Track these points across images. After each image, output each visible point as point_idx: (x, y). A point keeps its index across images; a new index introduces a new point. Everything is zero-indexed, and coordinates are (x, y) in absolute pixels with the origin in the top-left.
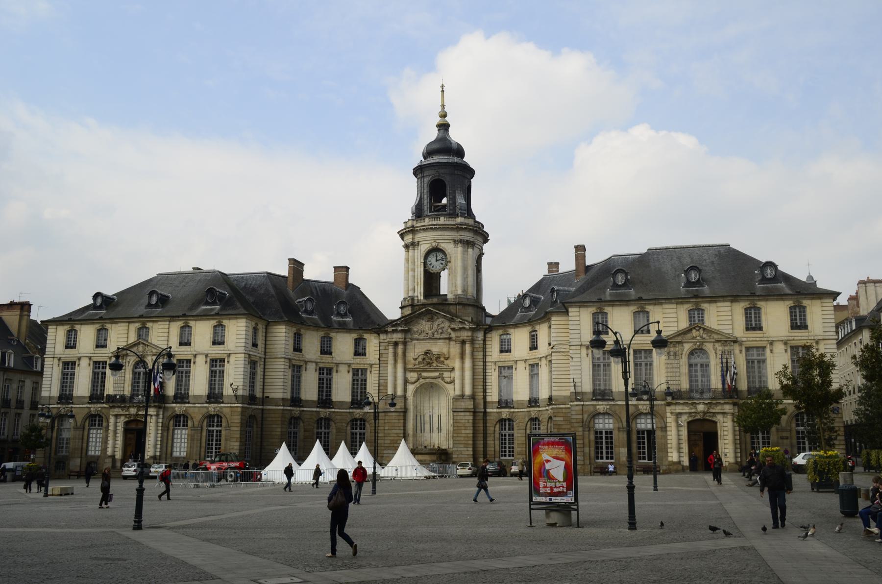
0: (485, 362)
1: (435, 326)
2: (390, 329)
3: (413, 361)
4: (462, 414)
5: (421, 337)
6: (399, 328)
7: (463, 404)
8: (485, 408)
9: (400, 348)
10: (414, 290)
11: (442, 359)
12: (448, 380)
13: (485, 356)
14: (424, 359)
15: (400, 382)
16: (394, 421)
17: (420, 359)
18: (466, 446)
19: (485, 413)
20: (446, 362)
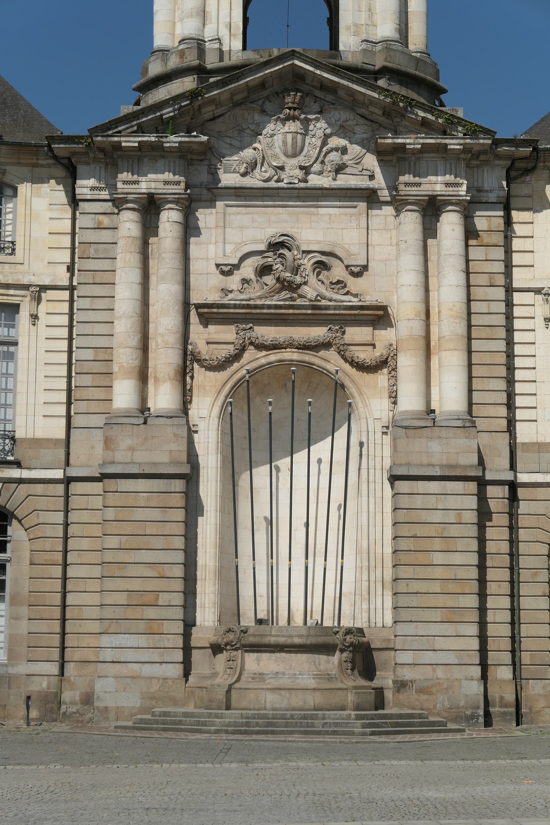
0: (509, 290)
1: (313, 142)
2: (130, 142)
3: (217, 280)
4: (434, 486)
5: (253, 181)
6: (173, 140)
7: (435, 447)
8: (513, 467)
9: (169, 219)
10: (203, 14)
11: (338, 272)
12: (364, 355)
13: (509, 266)
14: (264, 270)
15: (165, 357)
16: (140, 514)
17: (248, 270)
18: (452, 617)
19: (513, 486)
20: (354, 284)
